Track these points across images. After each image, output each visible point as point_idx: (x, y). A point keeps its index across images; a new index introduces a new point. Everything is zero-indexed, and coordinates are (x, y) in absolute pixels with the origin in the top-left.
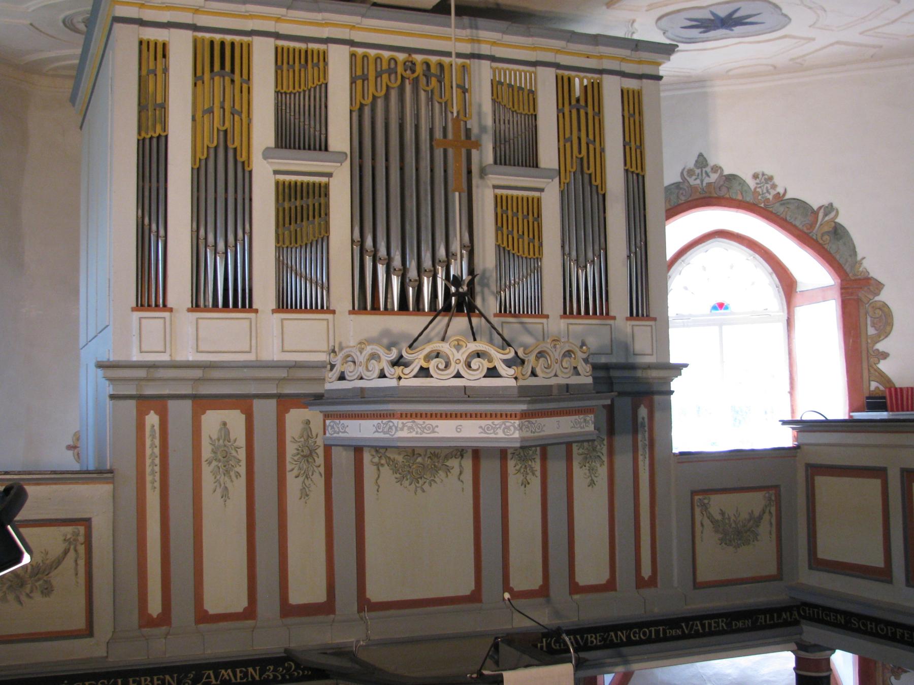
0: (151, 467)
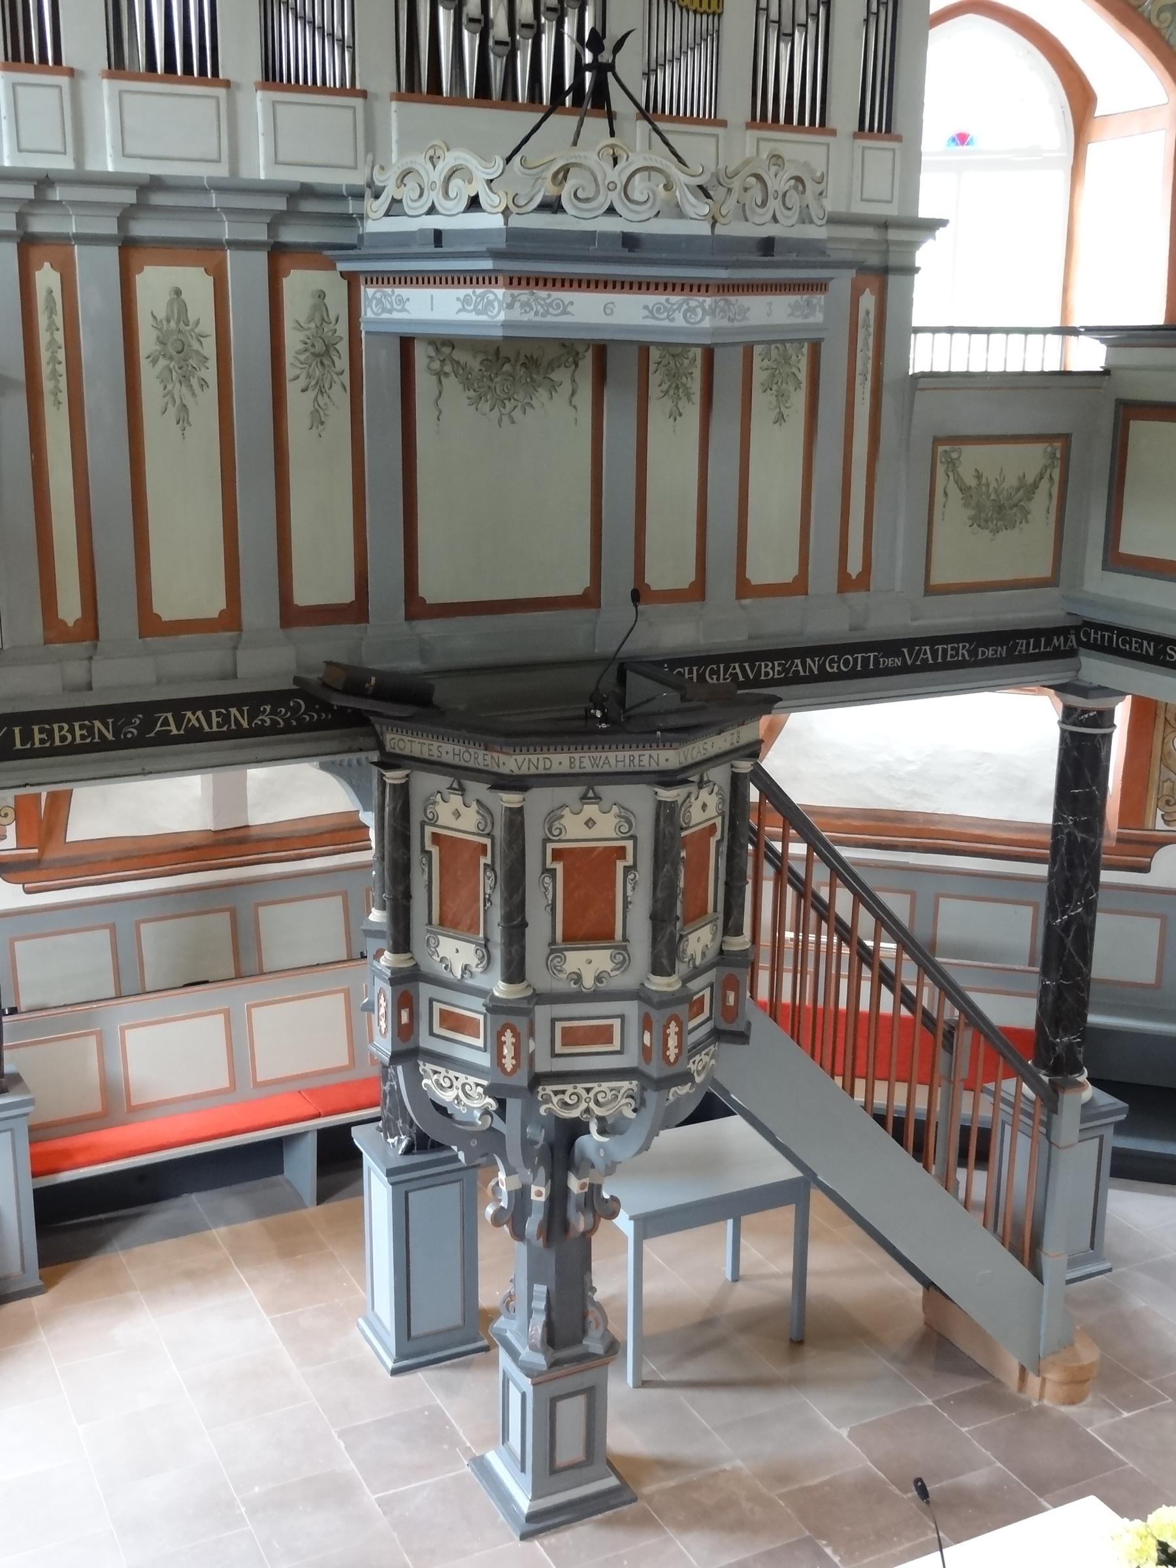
0: (51, 366)
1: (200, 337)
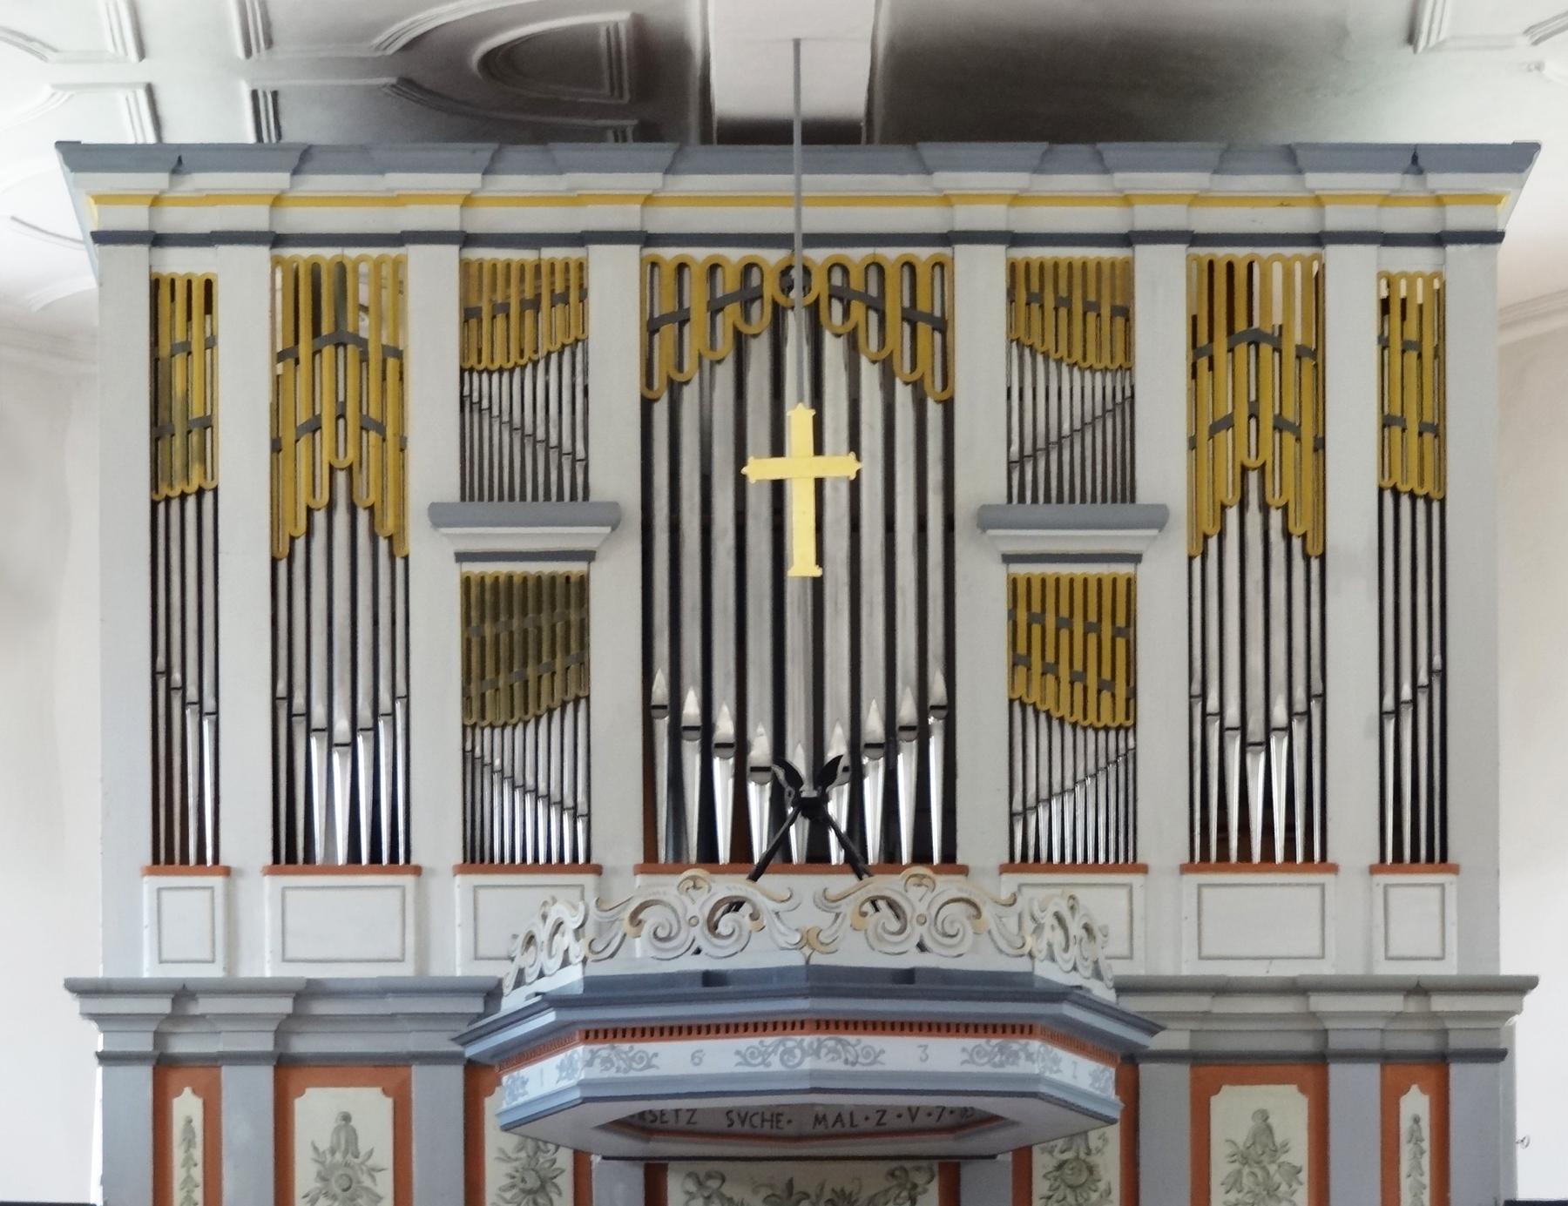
1: (372, 1171)
